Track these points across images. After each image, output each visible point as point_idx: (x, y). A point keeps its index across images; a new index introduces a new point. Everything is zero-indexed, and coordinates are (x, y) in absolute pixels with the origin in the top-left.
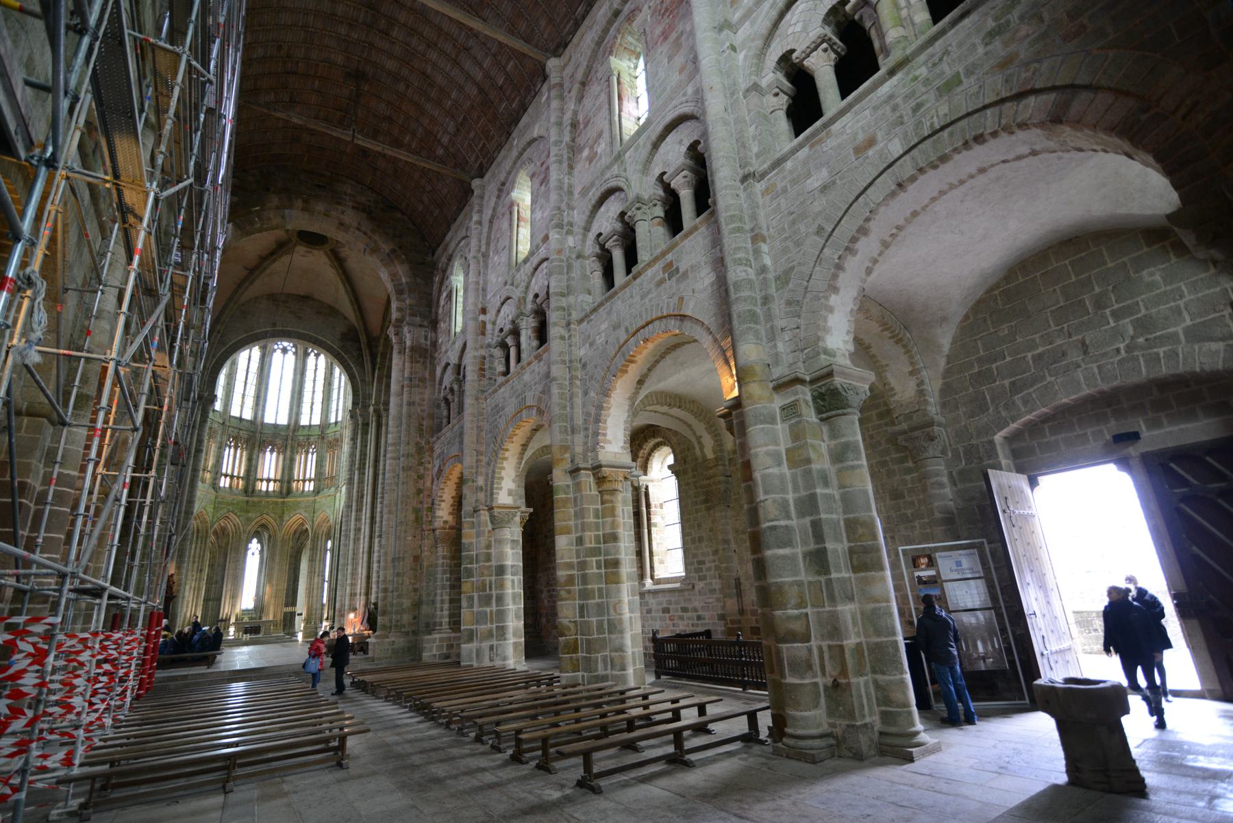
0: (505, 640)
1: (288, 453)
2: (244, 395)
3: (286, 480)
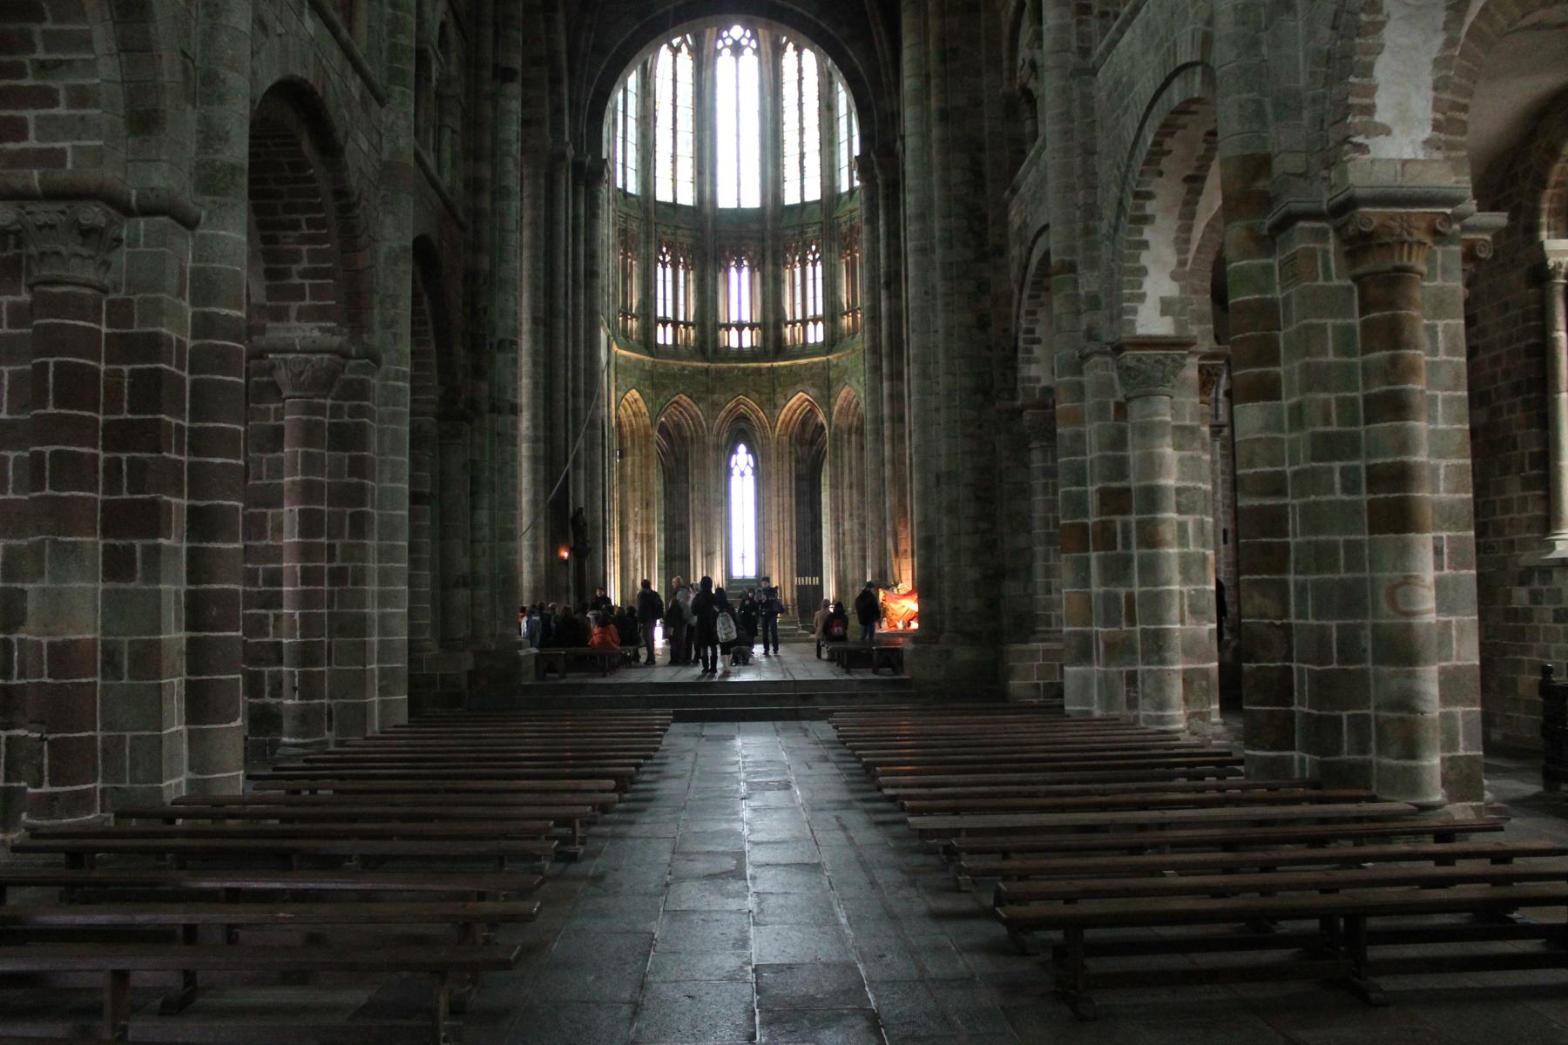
0: (1162, 661)
2: (674, 157)
3: (771, 320)
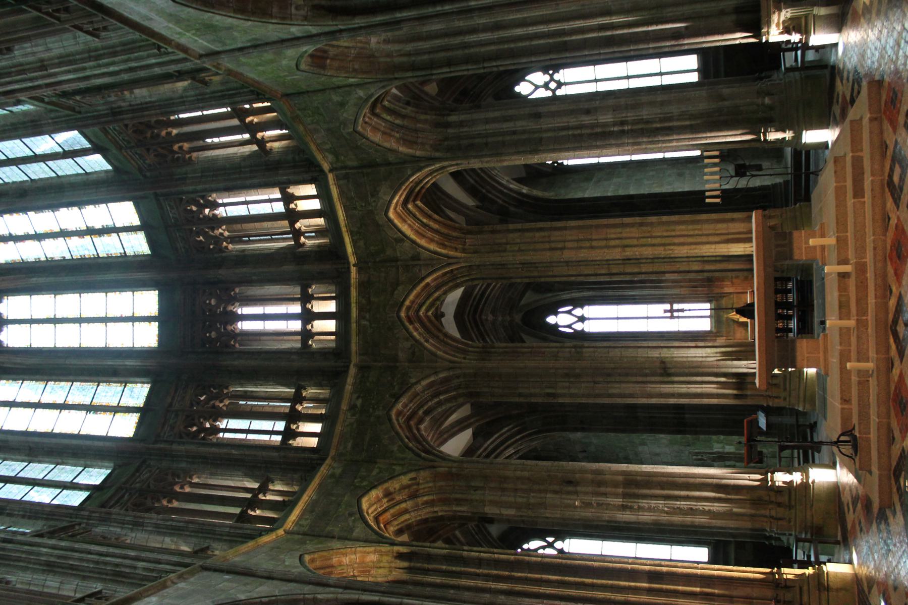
2: (91, 408)
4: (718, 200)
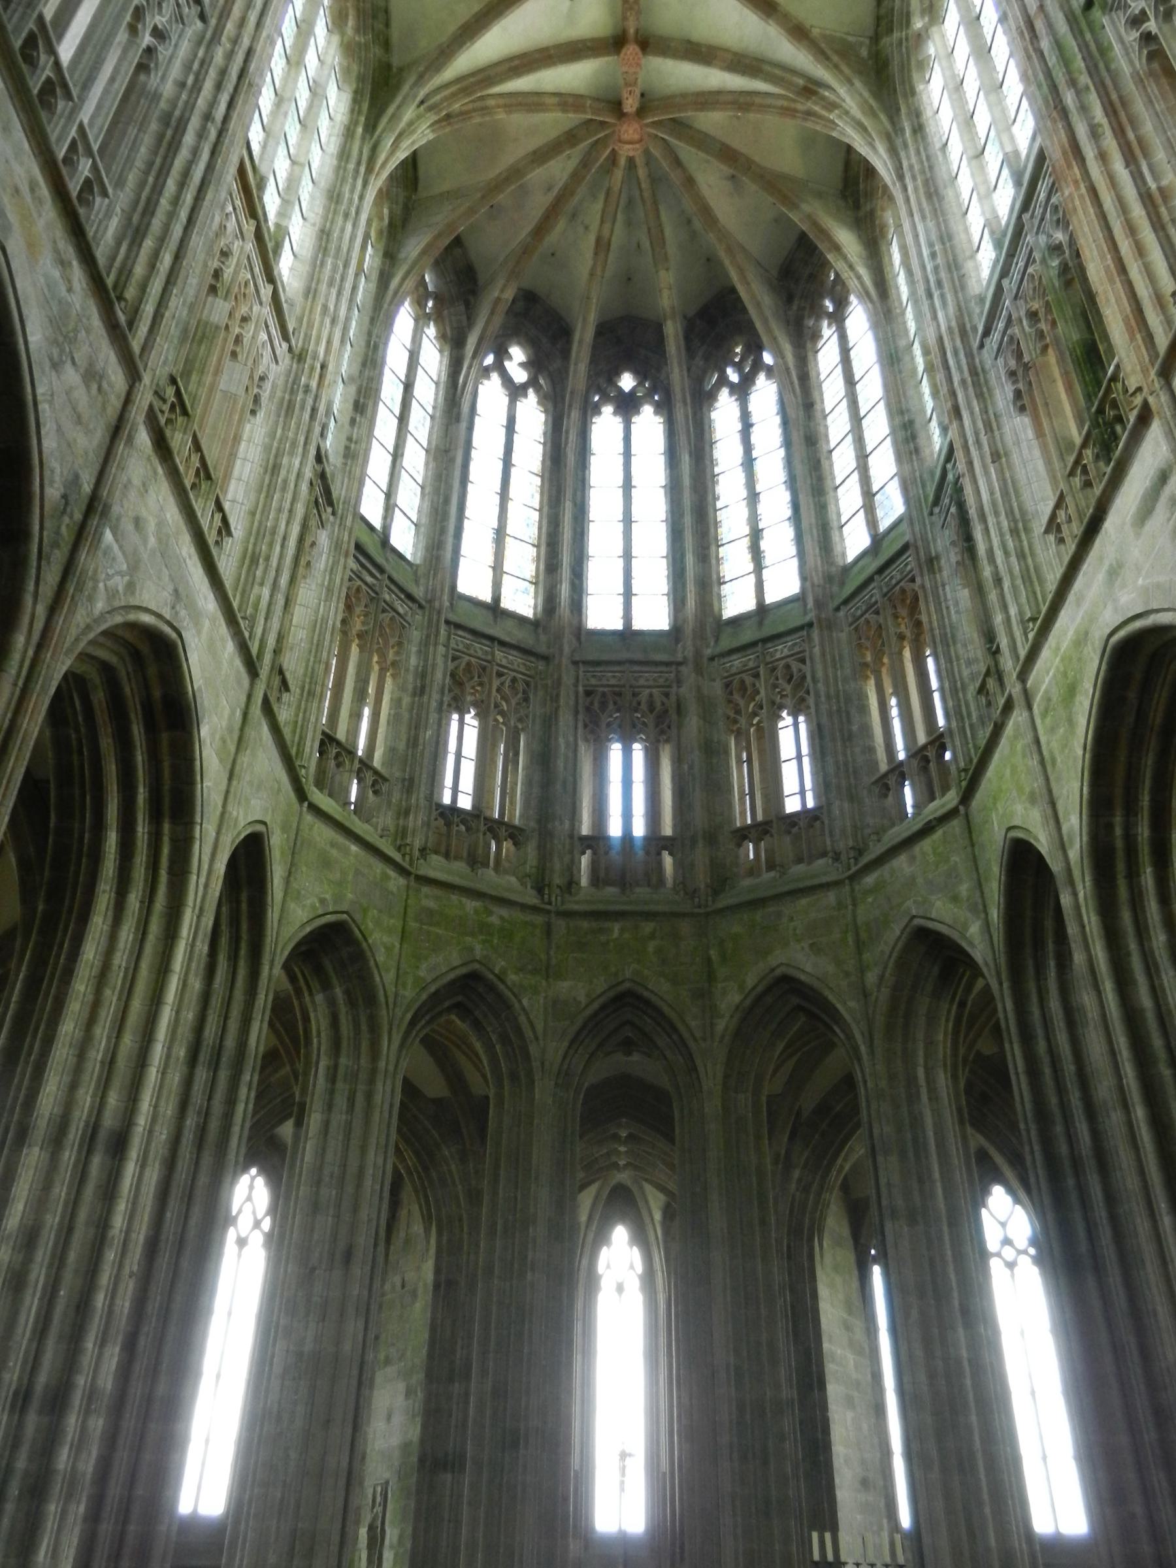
1: (693, 723)
2: (500, 535)
4: (816, 1556)
